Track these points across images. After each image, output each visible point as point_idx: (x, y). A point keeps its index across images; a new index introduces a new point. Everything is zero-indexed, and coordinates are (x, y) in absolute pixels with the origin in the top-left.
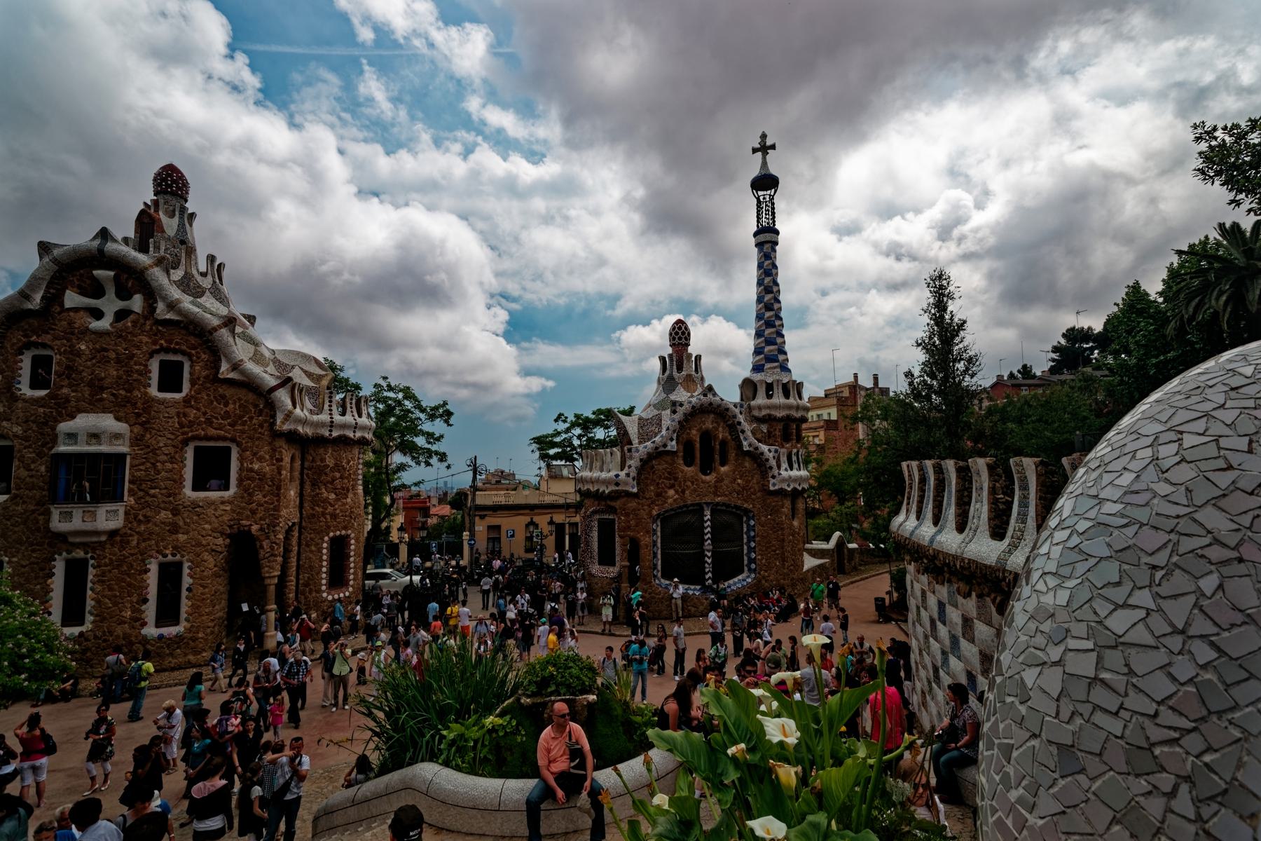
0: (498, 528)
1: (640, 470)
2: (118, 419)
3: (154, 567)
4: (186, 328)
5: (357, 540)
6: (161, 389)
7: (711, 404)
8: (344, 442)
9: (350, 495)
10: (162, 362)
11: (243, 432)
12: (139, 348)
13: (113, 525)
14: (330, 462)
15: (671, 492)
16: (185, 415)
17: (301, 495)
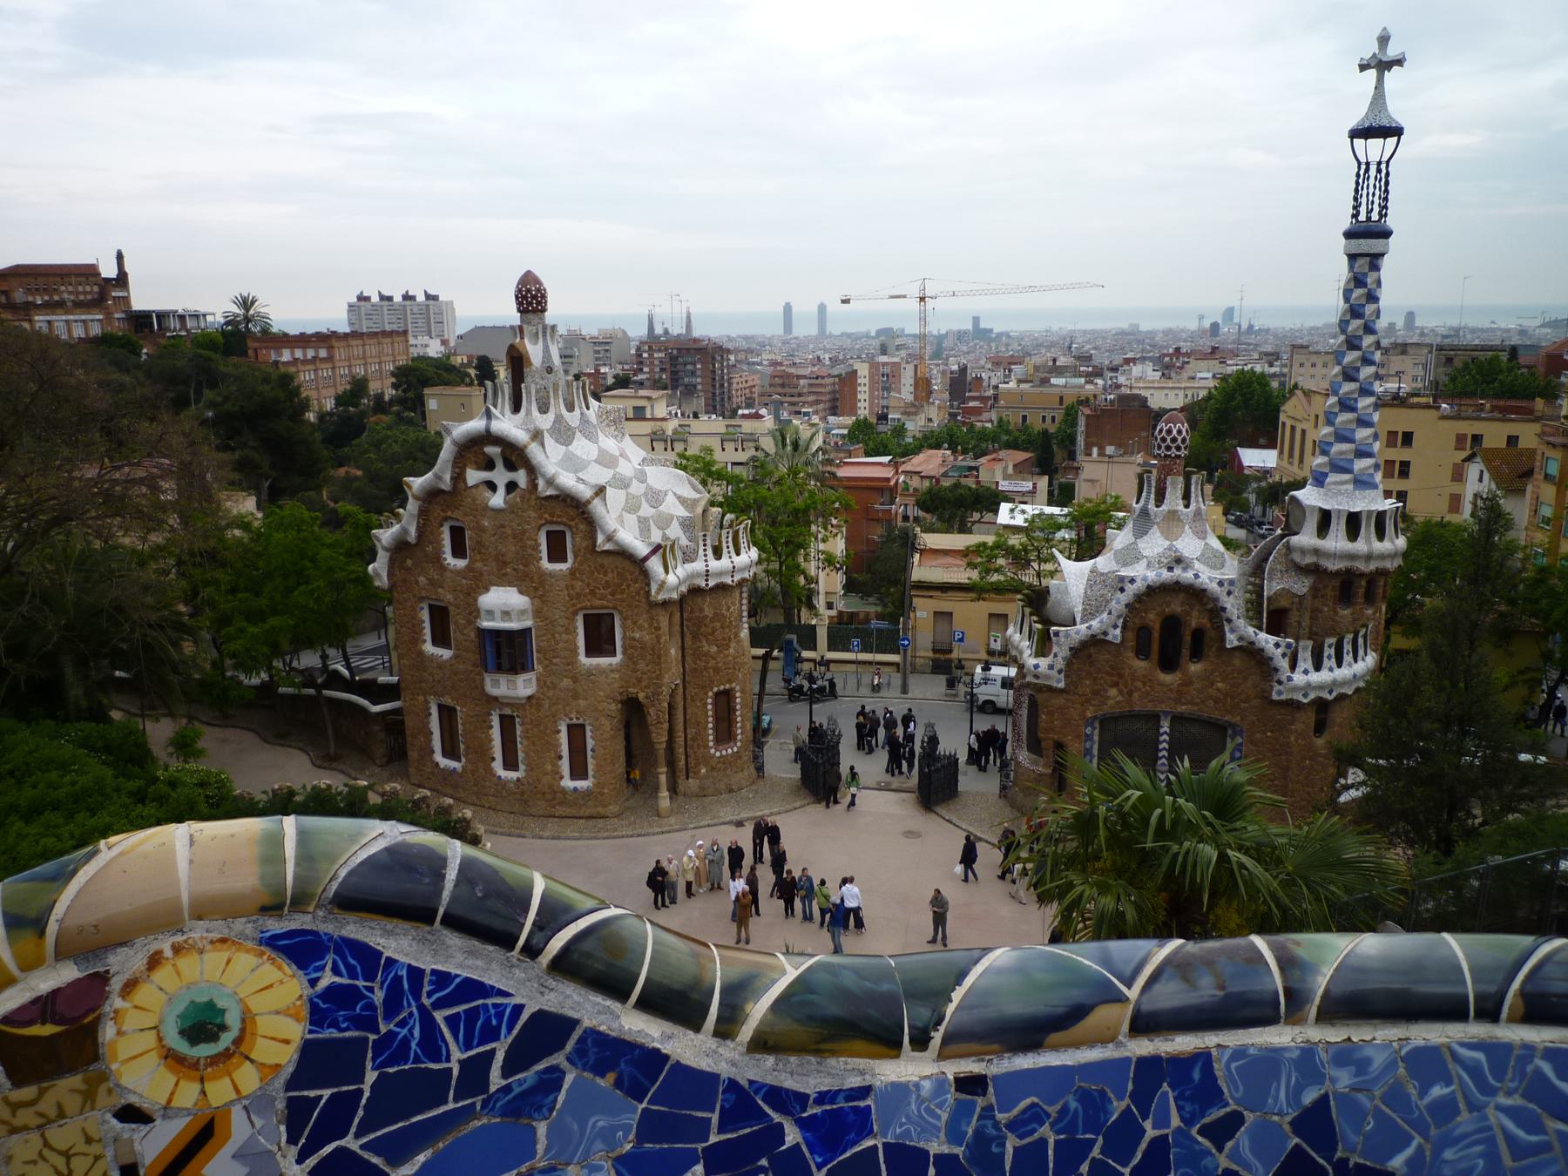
0: (951, 614)
1: (1069, 663)
2: (521, 592)
3: (564, 729)
4: (564, 500)
5: (743, 692)
6: (551, 560)
7: (1177, 583)
8: (722, 588)
9: (733, 645)
10: (548, 533)
11: (622, 600)
12: (529, 523)
13: (529, 692)
14: (708, 612)
15: (1113, 692)
16: (573, 587)
17: (683, 649)
